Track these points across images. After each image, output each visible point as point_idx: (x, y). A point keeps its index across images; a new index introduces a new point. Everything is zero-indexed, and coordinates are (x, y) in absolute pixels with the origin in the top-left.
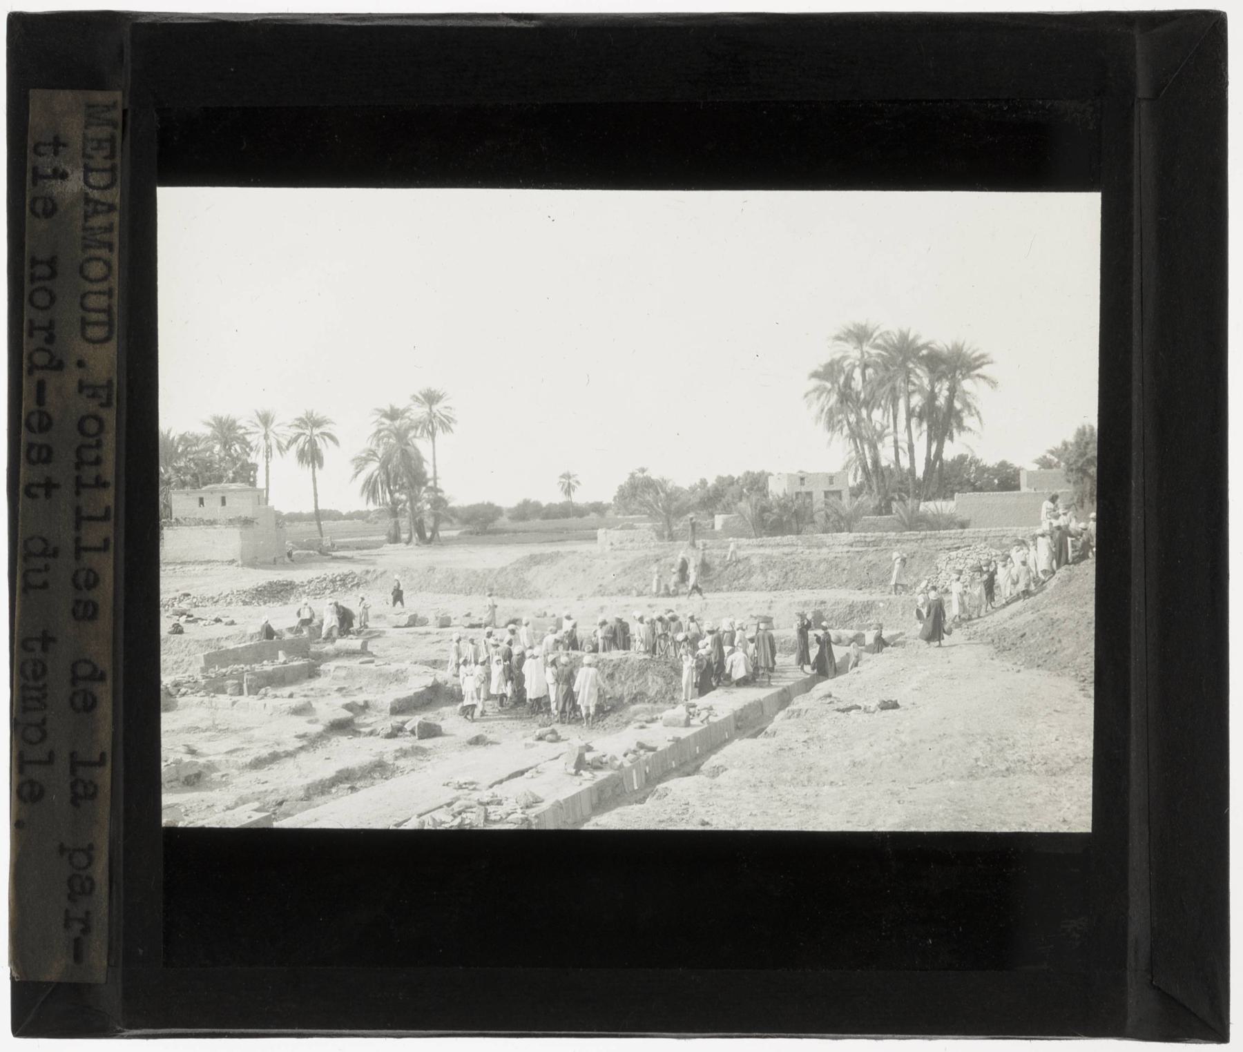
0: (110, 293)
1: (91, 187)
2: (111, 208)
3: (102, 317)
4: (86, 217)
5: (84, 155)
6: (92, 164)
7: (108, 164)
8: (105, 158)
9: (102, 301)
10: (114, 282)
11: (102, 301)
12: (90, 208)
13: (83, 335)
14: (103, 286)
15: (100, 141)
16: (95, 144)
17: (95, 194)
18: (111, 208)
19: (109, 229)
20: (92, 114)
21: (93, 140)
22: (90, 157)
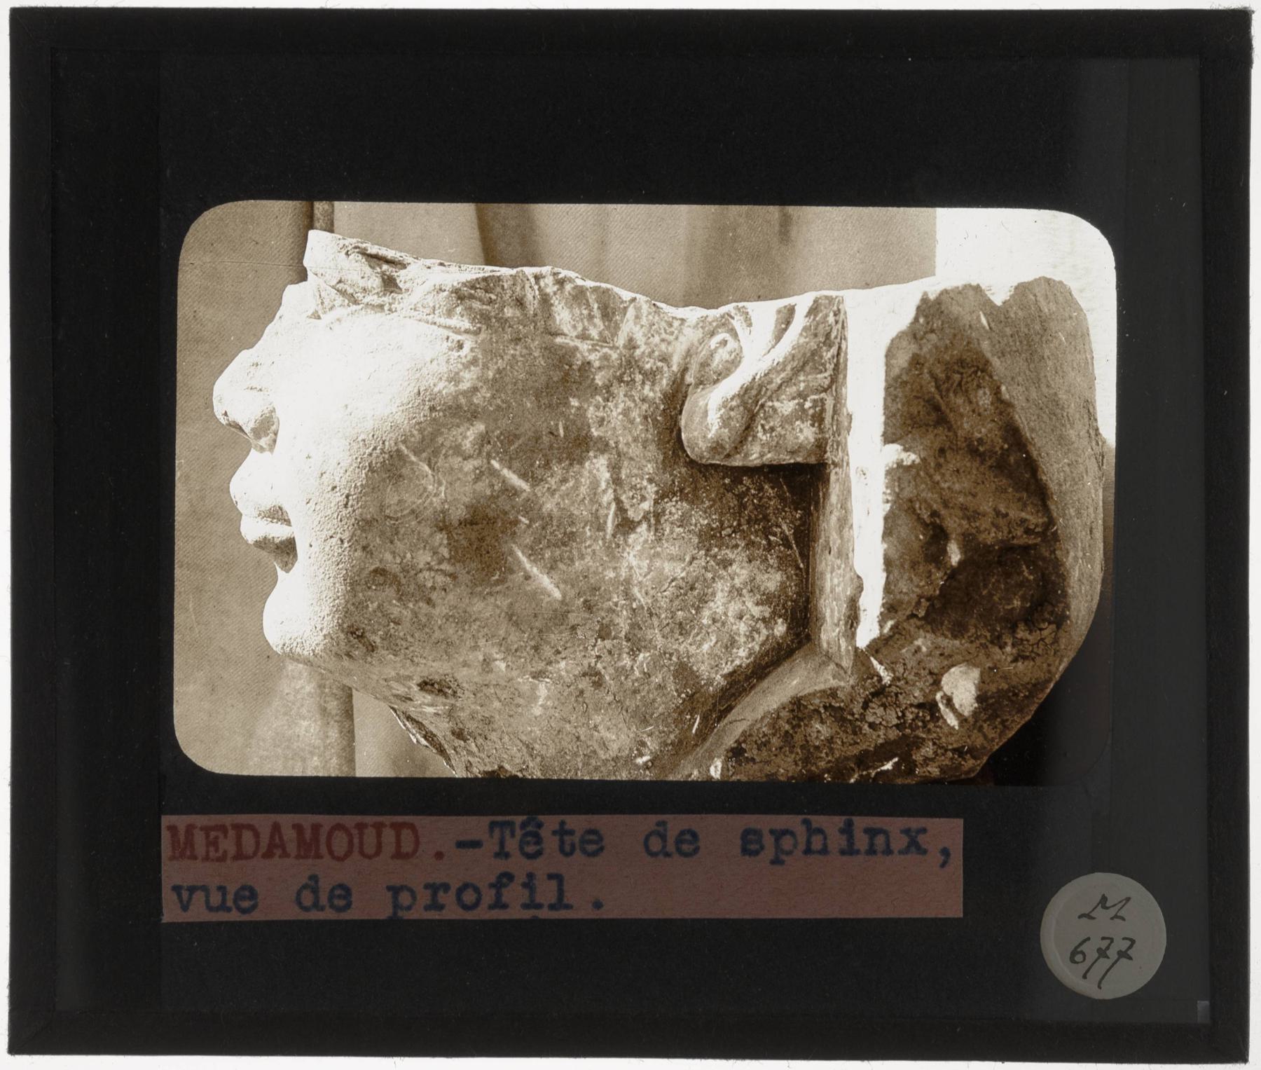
0: (361, 827)
1: (255, 853)
2: (276, 828)
3: (389, 836)
4: (285, 855)
5: (222, 859)
6: (232, 850)
7: (231, 833)
8: (226, 837)
9: (370, 834)
10: (349, 820)
11: (370, 834)
12: (278, 852)
13: (406, 856)
14: (355, 832)
15: (209, 844)
16: (212, 849)
17: (263, 849)
18: (276, 828)
19: (298, 828)
20: (185, 850)
21: (208, 852)
22: (225, 852)
